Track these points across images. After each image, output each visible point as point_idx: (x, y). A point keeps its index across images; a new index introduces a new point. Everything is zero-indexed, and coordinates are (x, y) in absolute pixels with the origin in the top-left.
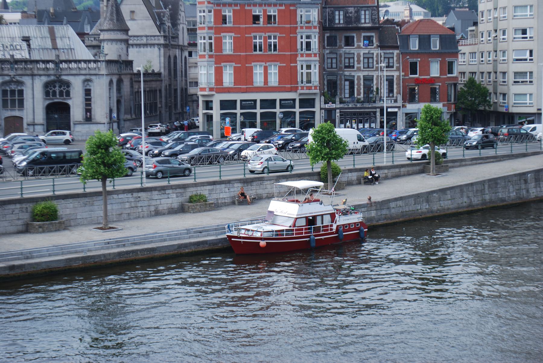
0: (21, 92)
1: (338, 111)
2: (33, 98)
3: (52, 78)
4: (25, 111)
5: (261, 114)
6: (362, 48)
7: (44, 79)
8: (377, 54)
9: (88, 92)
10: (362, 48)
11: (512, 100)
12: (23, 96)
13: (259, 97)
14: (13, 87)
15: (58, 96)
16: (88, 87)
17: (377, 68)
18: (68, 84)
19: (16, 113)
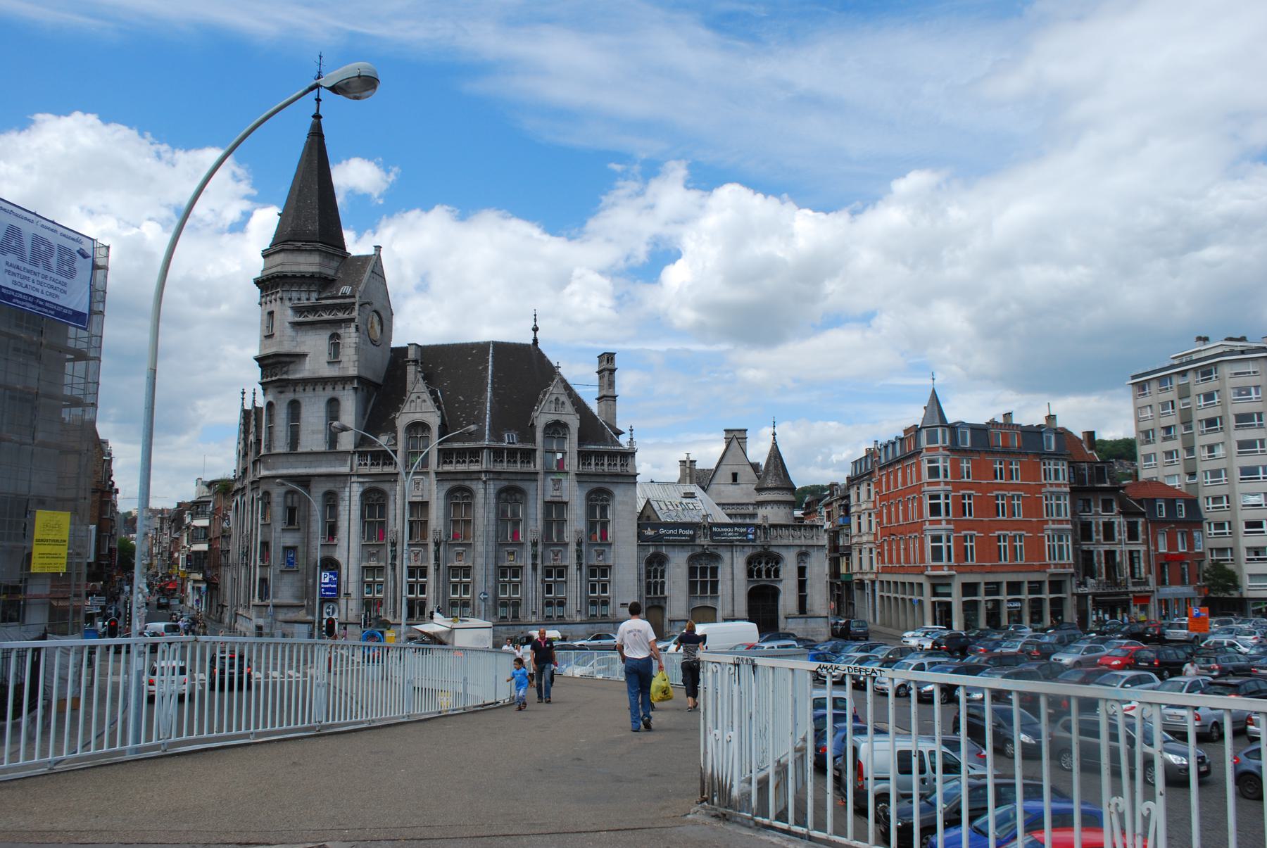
0: (714, 571)
1: (1090, 597)
2: (733, 579)
3: (759, 549)
4: (720, 599)
5: (1051, 600)
6: (1100, 515)
7: (749, 552)
8: (1119, 522)
9: (802, 571)
10: (1100, 515)
11: (1246, 582)
12: (716, 577)
13: (1004, 578)
14: (704, 563)
15: (764, 577)
16: (802, 564)
17: (1120, 540)
18: (777, 559)
19: (709, 603)
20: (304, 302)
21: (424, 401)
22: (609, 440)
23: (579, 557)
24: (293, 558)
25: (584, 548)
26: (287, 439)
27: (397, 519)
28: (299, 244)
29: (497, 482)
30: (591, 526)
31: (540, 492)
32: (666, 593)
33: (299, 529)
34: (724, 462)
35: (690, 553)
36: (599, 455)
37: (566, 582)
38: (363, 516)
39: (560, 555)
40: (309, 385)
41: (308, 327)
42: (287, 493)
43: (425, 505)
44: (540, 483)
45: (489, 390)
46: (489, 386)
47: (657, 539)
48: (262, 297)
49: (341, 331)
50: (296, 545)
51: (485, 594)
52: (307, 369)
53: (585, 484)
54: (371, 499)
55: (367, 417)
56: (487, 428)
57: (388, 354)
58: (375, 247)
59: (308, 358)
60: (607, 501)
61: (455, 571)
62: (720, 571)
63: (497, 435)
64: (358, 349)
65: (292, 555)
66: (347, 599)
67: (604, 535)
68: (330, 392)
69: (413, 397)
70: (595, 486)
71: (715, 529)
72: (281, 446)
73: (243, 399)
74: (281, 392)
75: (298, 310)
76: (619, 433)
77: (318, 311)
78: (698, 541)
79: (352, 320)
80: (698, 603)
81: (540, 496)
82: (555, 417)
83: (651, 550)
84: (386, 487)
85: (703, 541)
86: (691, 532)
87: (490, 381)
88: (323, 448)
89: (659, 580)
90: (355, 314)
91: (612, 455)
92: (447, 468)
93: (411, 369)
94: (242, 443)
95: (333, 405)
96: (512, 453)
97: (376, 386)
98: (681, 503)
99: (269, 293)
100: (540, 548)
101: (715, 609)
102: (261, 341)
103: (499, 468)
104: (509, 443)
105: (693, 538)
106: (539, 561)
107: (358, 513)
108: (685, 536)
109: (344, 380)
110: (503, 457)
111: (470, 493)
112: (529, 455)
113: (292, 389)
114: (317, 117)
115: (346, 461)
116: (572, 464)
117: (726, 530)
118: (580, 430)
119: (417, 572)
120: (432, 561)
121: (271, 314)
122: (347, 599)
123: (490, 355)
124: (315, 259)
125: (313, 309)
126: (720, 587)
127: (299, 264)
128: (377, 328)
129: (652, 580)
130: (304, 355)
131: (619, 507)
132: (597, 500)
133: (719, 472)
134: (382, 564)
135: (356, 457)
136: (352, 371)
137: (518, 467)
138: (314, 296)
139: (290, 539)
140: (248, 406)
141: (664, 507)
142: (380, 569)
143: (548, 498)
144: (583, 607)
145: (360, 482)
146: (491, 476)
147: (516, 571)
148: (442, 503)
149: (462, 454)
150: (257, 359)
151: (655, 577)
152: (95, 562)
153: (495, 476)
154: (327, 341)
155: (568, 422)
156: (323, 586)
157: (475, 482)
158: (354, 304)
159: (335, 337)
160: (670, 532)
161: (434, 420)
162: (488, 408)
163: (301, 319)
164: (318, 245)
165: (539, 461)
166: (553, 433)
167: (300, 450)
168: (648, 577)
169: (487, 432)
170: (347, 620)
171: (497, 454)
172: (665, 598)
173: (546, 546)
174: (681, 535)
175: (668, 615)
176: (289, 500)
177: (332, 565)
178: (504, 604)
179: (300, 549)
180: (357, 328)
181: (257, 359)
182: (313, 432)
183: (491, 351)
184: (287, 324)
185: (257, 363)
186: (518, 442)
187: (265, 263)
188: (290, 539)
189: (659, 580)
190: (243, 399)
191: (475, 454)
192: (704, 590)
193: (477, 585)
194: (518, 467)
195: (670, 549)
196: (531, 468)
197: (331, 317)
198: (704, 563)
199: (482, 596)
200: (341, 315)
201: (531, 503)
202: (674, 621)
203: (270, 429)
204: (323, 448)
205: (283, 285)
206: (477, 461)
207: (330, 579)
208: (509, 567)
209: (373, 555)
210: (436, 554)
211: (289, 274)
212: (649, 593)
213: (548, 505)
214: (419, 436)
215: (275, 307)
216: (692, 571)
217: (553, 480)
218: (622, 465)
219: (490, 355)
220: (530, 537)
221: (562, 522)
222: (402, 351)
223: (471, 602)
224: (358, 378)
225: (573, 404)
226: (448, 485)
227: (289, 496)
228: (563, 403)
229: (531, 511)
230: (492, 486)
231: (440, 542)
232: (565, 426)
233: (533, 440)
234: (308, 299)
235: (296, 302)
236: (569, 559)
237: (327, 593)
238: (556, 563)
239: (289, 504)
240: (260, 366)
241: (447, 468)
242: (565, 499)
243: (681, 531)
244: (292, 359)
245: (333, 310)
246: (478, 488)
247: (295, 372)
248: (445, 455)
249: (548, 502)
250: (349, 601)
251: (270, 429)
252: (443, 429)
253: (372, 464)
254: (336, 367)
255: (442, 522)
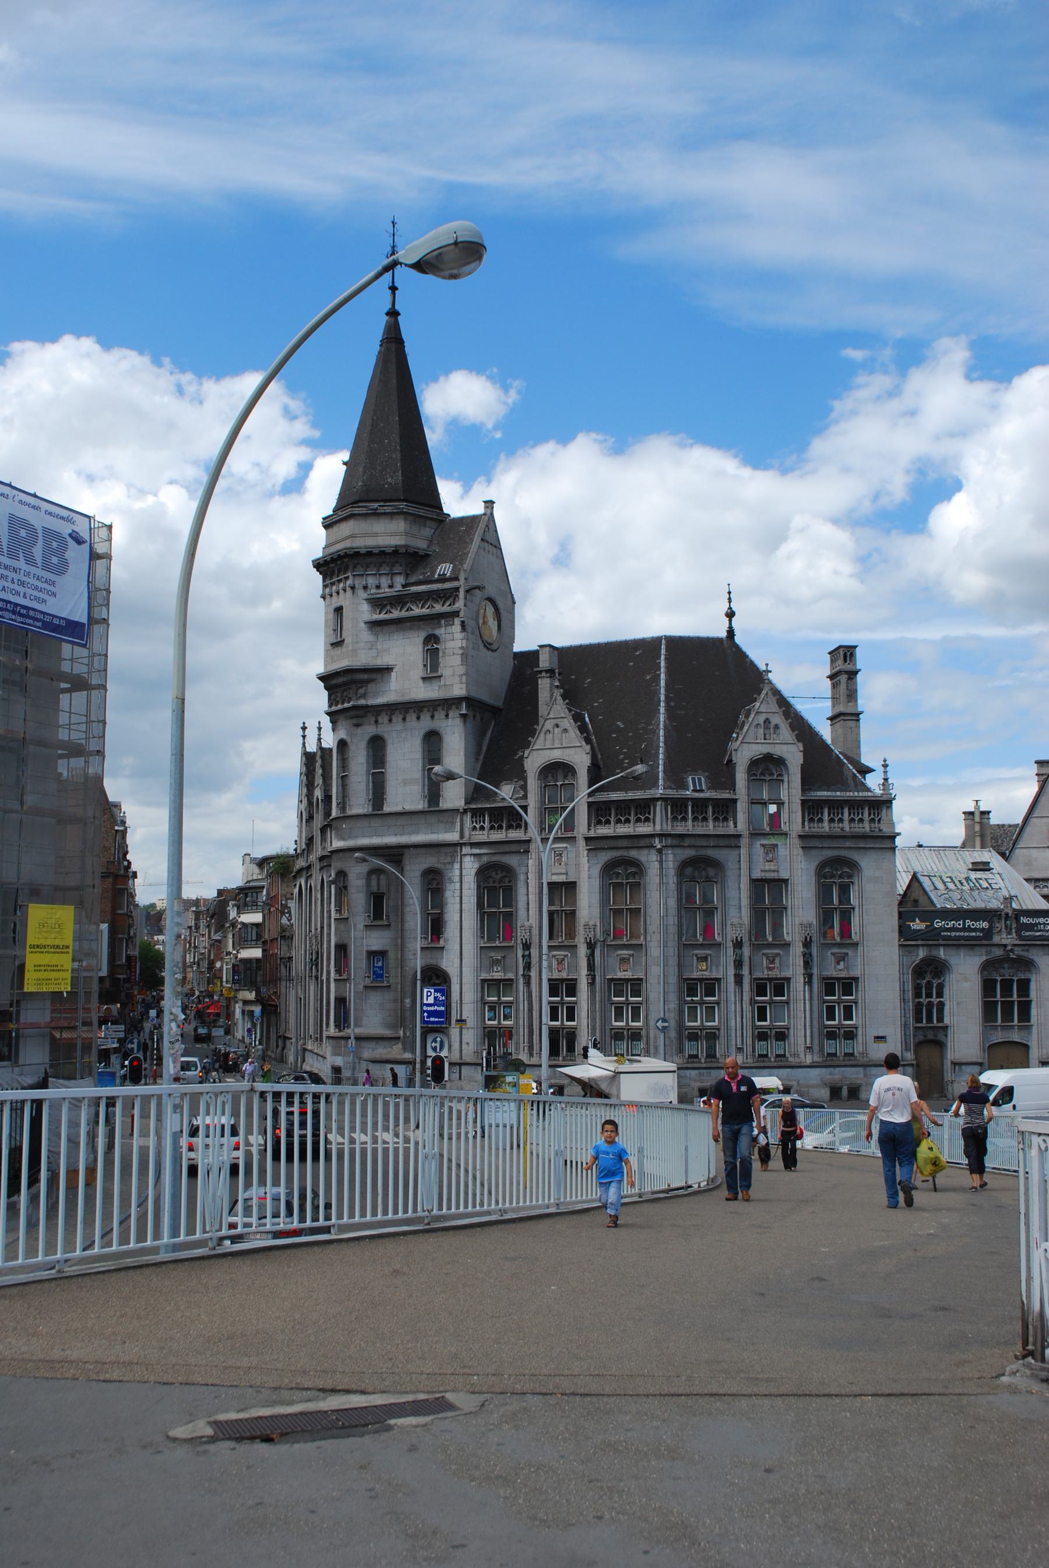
0: (1024, 986)
4: (1034, 1030)
12: (1028, 996)
14: (1007, 973)
19: (1016, 1036)
20: (385, 591)
21: (566, 731)
22: (851, 782)
23: (807, 964)
24: (381, 968)
25: (814, 951)
26: (368, 794)
28: (375, 505)
29: (678, 851)
30: (826, 917)
31: (744, 865)
32: (947, 1020)
33: (389, 925)
34: (1036, 813)
35: (984, 958)
36: (836, 806)
37: (787, 1003)
38: (480, 905)
39: (777, 961)
40: (397, 712)
41: (392, 628)
42: (371, 872)
43: (571, 887)
44: (743, 851)
45: (662, 710)
46: (662, 704)
47: (931, 936)
48: (325, 586)
49: (440, 632)
50: (385, 948)
51: (664, 1020)
52: (393, 691)
53: (814, 852)
54: (491, 880)
55: (482, 757)
56: (661, 768)
57: (511, 663)
58: (485, 502)
59: (393, 674)
60: (850, 876)
61: (617, 985)
62: (1033, 986)
63: (676, 779)
64: (465, 656)
65: (380, 964)
66: (461, 1028)
67: (846, 931)
68: (426, 723)
69: (549, 725)
70: (829, 854)
71: (1024, 920)
72: (359, 804)
73: (304, 737)
74: (357, 725)
75: (377, 603)
76: (866, 770)
77: (405, 603)
78: (996, 939)
79: (456, 614)
80: (998, 1037)
81: (744, 871)
82: (765, 749)
83: (922, 953)
84: (512, 861)
85: (1005, 938)
86: (985, 925)
87: (662, 698)
88: (420, 805)
89: (935, 1000)
90: (460, 604)
91: (856, 805)
92: (603, 831)
93: (544, 684)
94: (305, 801)
95: (432, 741)
96: (700, 806)
97: (493, 710)
98: (968, 879)
99: (335, 579)
100: (746, 951)
101: (1026, 1047)
102: (326, 651)
103: (680, 829)
104: (695, 790)
105: (988, 934)
106: (745, 971)
107: (474, 900)
108: (975, 930)
109: (447, 704)
110: (686, 812)
111: (637, 868)
112: (725, 809)
113: (373, 719)
114: (393, 313)
115: (453, 823)
116: (794, 820)
117: (1041, 920)
118: (804, 769)
119: (559, 987)
120: (584, 971)
121: (339, 610)
122: (461, 1028)
123: (663, 657)
124: (399, 525)
125: (399, 601)
126: (1034, 1012)
127: (376, 535)
128: (493, 624)
129: (924, 1000)
130: (388, 670)
131: (868, 887)
132: (833, 876)
133: (1028, 829)
134: (510, 976)
135: (468, 818)
136: (459, 690)
137: (711, 827)
138: (399, 580)
139: (377, 941)
140: (312, 747)
141: (940, 886)
142: (507, 984)
143: (757, 874)
144: (816, 1041)
145: (475, 855)
146: (669, 841)
147: (711, 986)
148: (596, 883)
149: (623, 810)
150: (322, 678)
151: (929, 995)
152: (109, 976)
153: (675, 842)
154: (421, 647)
155: (785, 756)
156: (425, 1008)
157: (645, 852)
158: (457, 589)
159: (431, 640)
160: (951, 924)
161: (580, 759)
162: (662, 739)
163: (383, 616)
164: (402, 505)
165: (741, 817)
166: (762, 774)
167: (387, 809)
168: (917, 994)
169: (661, 775)
170: (461, 1058)
171: (677, 807)
172: (945, 1028)
173: (756, 947)
174: (969, 930)
175: (950, 1056)
176: (374, 883)
177: (438, 977)
178: (693, 1037)
179: (391, 955)
180: (463, 625)
181: (322, 678)
182: (405, 783)
183: (663, 651)
184: (363, 625)
185: (322, 684)
186: (709, 788)
187: (327, 536)
188: (377, 941)
189: (935, 1000)
190: (304, 737)
191: (643, 809)
192: (1008, 1016)
193: (652, 1008)
194: (711, 827)
195: (952, 951)
196: (730, 828)
197: (425, 611)
198: (1007, 973)
199: (660, 1024)
200: (439, 608)
201: (731, 882)
202: (960, 1064)
203: (344, 779)
204: (420, 805)
205: (355, 567)
206: (647, 820)
207: (435, 998)
208: (701, 980)
209: (495, 962)
210: (589, 960)
211: (363, 551)
212: (918, 1019)
213: (758, 885)
214: (559, 783)
215: (345, 600)
216: (988, 986)
217: (763, 845)
218: (872, 821)
219: (663, 657)
220: (731, 934)
221: (779, 911)
222: (529, 658)
223: (643, 1033)
224: (468, 700)
225: (793, 727)
226: (605, 857)
227: (374, 877)
228: (777, 727)
229: (732, 894)
230: (671, 857)
231: (595, 943)
233: (732, 786)
234: (391, 587)
235: (373, 591)
236: (793, 967)
237: (432, 1019)
238: (773, 974)
239: (374, 889)
240: (326, 688)
241: (603, 831)
242: (784, 875)
243: (968, 922)
244: (373, 676)
245: (427, 601)
246: (650, 860)
247: (376, 694)
248: (599, 812)
249: (757, 880)
250: (464, 1031)
251: (344, 779)
252: (595, 773)
253: (492, 828)
254: (435, 685)
255: (596, 911)
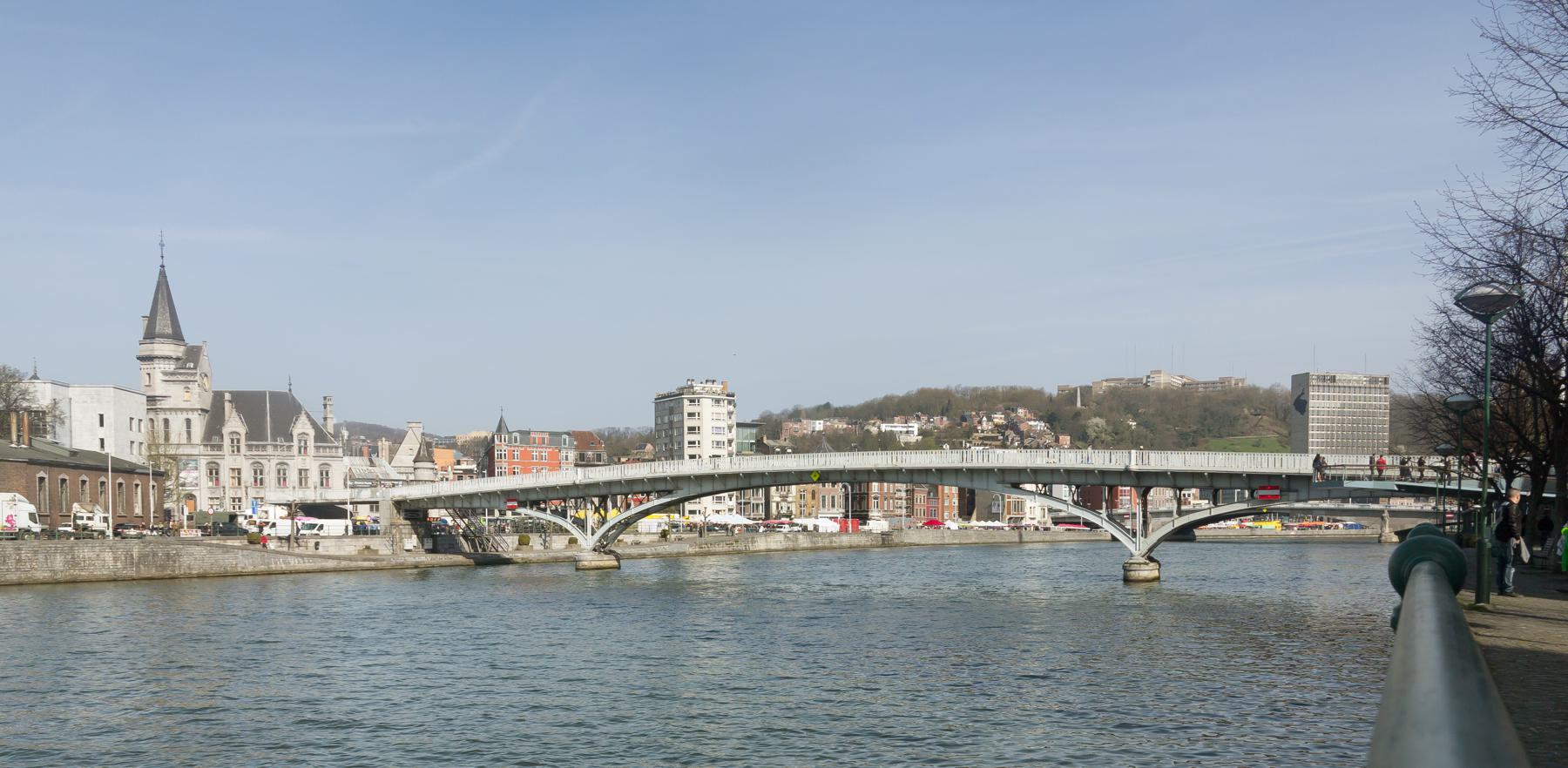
27: (225, 476)
36: (325, 448)
68: (185, 415)
75: (165, 374)
84: (218, 461)
93: (227, 405)
112: (290, 447)
125: (172, 374)
135: (202, 447)
143: (300, 468)
161: (242, 430)
163: (166, 378)
194: (286, 453)
200: (189, 378)
232: (307, 434)
